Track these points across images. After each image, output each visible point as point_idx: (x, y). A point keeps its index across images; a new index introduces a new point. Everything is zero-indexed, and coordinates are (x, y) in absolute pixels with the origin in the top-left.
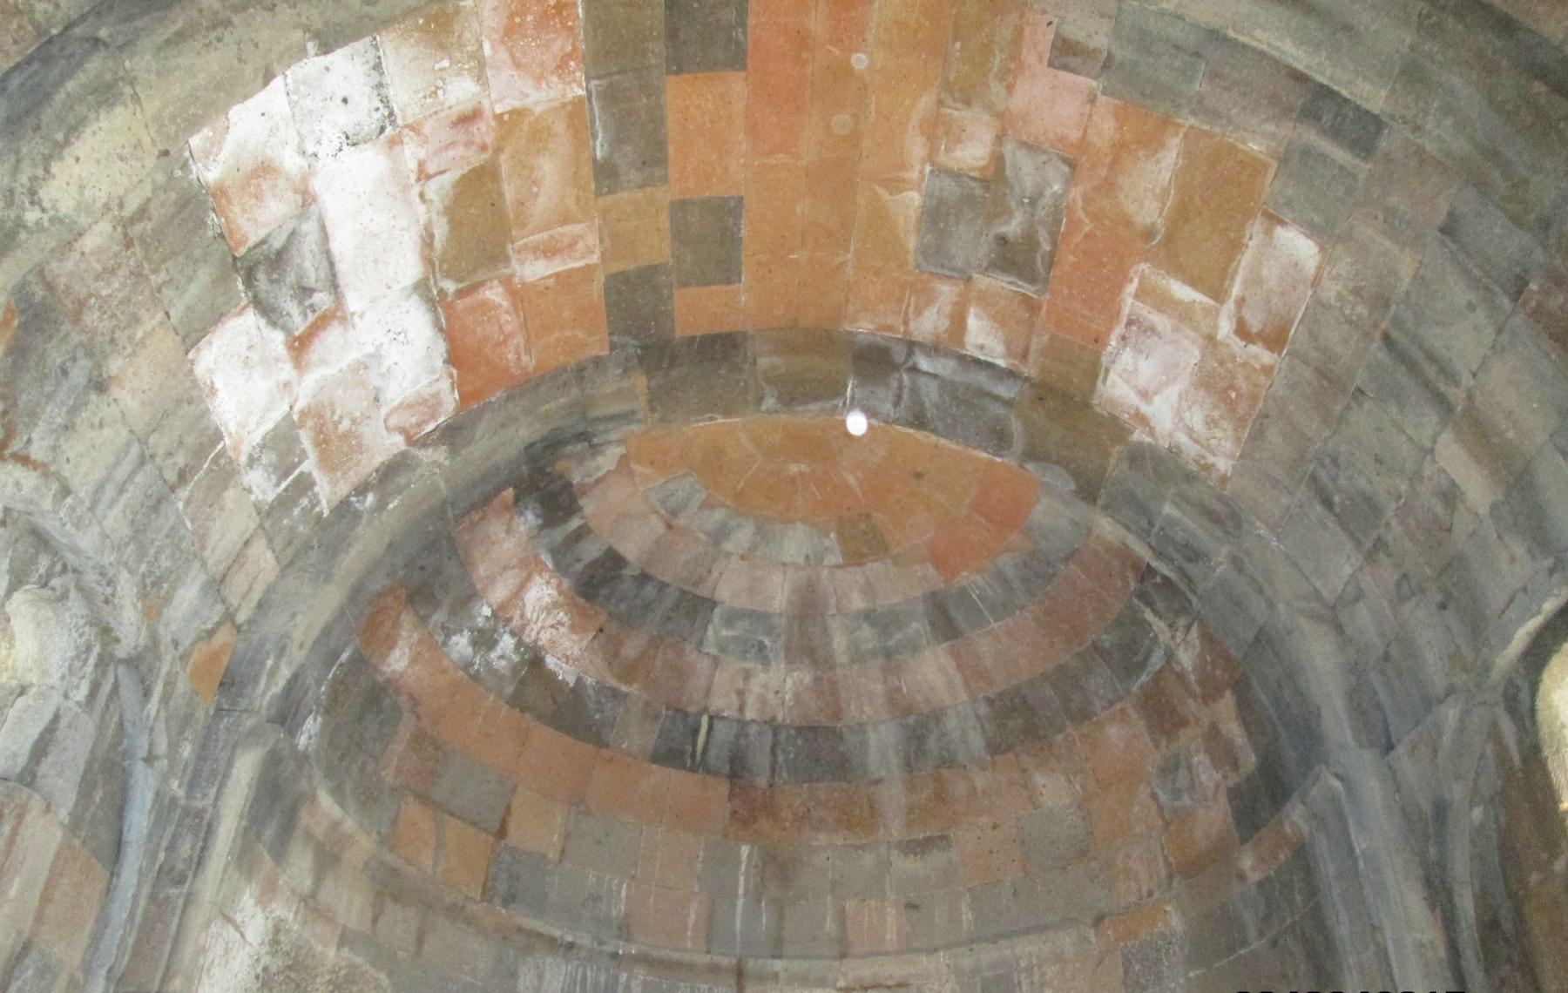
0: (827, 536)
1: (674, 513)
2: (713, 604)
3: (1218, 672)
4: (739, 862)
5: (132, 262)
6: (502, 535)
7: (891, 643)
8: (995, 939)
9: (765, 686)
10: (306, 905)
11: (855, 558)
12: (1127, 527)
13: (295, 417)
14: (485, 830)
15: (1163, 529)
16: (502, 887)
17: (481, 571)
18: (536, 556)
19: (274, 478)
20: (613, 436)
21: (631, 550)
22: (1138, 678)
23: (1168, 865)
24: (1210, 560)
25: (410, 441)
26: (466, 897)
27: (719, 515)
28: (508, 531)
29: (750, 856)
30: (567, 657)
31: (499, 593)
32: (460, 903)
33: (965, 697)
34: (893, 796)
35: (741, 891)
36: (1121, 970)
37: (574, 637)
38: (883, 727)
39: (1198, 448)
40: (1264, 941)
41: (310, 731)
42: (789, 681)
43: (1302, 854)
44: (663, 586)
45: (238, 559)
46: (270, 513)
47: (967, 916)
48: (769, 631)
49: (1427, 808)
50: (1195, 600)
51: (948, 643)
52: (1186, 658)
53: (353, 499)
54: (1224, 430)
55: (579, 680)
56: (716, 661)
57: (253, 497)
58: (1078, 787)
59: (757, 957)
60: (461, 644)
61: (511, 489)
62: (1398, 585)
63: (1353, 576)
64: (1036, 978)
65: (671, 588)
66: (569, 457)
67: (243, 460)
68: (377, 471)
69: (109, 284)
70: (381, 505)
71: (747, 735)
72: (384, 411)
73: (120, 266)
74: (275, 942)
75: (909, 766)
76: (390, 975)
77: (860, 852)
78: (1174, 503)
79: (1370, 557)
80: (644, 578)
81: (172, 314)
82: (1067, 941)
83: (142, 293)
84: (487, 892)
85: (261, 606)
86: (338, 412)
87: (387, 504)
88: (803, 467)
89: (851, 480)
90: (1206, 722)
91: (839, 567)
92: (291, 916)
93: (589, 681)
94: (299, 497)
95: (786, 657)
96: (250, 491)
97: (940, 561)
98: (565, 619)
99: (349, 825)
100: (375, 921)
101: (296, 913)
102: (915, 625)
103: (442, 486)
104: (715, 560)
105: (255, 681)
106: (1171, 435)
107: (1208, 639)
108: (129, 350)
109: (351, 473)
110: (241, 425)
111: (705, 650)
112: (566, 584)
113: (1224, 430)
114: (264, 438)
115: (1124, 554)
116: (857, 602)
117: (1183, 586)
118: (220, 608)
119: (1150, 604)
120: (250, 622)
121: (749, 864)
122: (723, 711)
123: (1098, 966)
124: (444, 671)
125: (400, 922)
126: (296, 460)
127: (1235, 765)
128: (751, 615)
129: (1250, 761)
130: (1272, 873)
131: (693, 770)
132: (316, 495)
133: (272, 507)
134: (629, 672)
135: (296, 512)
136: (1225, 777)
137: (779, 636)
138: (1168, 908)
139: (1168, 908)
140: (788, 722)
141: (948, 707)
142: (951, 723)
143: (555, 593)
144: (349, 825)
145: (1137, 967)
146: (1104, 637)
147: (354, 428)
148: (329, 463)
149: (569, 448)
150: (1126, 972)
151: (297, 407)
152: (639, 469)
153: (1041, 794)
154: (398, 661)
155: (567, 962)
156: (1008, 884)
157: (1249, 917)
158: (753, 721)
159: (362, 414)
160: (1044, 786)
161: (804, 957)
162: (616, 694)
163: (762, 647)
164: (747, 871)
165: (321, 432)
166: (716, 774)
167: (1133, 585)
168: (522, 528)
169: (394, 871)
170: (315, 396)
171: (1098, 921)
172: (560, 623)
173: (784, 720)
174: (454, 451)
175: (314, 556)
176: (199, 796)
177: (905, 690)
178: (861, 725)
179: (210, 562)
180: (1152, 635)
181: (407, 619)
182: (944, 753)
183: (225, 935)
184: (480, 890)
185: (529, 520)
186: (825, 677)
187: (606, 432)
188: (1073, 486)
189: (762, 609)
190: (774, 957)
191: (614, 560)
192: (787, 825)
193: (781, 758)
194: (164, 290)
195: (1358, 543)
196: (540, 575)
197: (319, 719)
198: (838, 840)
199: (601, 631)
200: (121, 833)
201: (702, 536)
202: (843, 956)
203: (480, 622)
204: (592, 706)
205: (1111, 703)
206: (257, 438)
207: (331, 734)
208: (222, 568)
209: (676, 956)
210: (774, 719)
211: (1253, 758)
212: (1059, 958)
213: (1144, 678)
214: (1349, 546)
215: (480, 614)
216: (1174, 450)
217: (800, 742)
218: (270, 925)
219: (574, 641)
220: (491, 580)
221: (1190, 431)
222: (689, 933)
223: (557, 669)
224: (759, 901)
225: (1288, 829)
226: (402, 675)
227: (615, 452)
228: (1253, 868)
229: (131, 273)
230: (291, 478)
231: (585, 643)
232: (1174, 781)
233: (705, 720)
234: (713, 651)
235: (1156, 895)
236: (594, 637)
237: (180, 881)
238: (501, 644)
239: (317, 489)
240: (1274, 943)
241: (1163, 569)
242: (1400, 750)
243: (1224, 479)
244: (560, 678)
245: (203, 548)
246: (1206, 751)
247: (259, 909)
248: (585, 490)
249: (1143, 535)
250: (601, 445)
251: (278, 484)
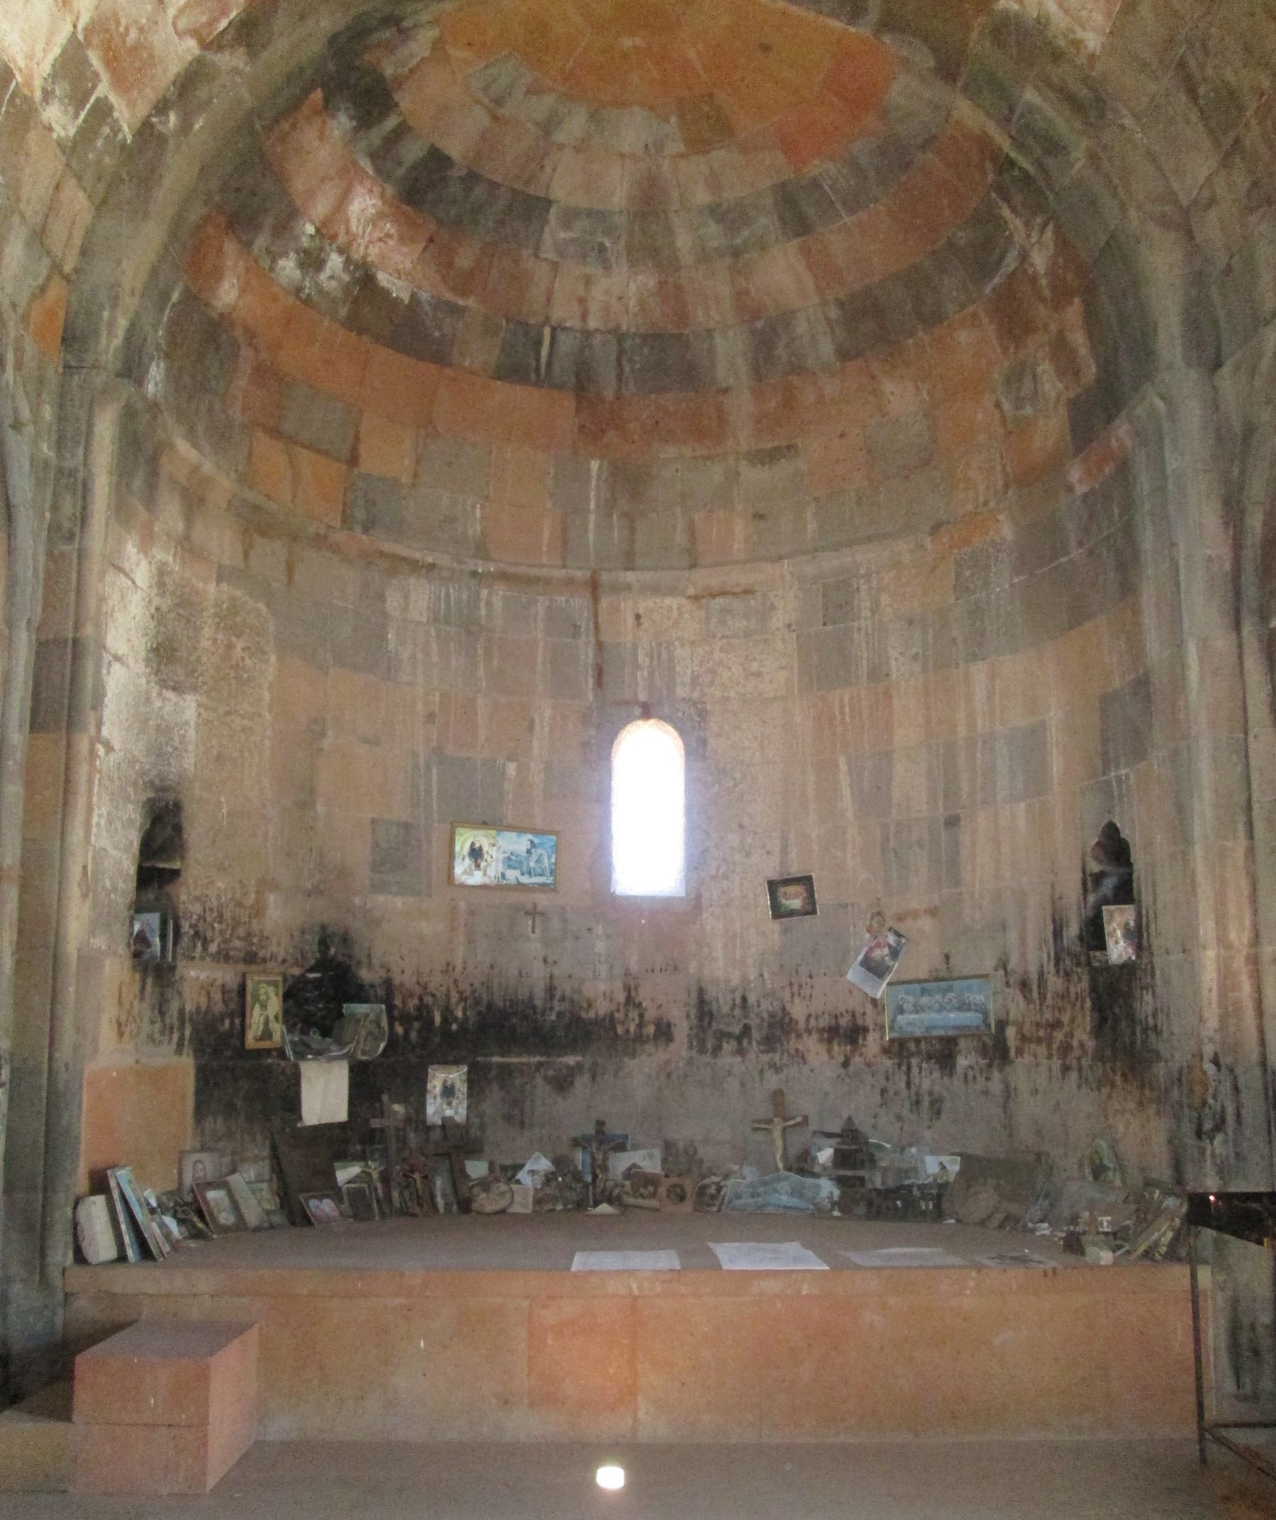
0: (667, 120)
1: (499, 102)
2: (549, 203)
3: (1069, 276)
4: (588, 480)
6: (316, 143)
7: (738, 241)
8: (837, 547)
9: (607, 292)
10: (182, 546)
11: (698, 145)
12: (988, 114)
13: (81, 37)
14: (338, 460)
15: (1022, 116)
16: (360, 514)
17: (299, 184)
18: (355, 163)
19: (71, 110)
20: (424, 17)
21: (455, 149)
22: (992, 278)
23: (1006, 475)
24: (1068, 154)
25: (205, 45)
26: (329, 527)
27: (549, 100)
28: (321, 138)
29: (600, 468)
30: (399, 273)
31: (321, 207)
32: (322, 532)
33: (815, 299)
34: (741, 406)
35: (592, 506)
36: (953, 575)
37: (405, 250)
38: (731, 333)
39: (1068, 19)
40: (1081, 551)
41: (156, 377)
42: (633, 286)
44: (495, 185)
45: (52, 207)
46: (72, 149)
47: (812, 526)
48: (609, 231)
49: (1238, 430)
51: (799, 239)
52: (1039, 261)
53: (154, 120)
55: (413, 295)
56: (555, 266)
57: (55, 135)
58: (925, 396)
59: (610, 570)
60: (288, 267)
61: (319, 90)
62: (1249, 192)
64: (874, 584)
65: (503, 189)
66: (378, 45)
67: (38, 94)
68: (174, 83)
70: (185, 127)
71: (591, 346)
72: (171, 12)
74: (161, 585)
75: (757, 373)
76: (267, 605)
77: (709, 463)
78: (1036, 87)
79: (1226, 162)
80: (472, 178)
82: (903, 547)
84: (347, 520)
85: (84, 252)
86: (124, 21)
87: (192, 125)
88: (638, 41)
89: (692, 53)
90: (1053, 328)
91: (682, 156)
92: (170, 559)
93: (424, 296)
94: (100, 125)
95: (629, 260)
96: (50, 129)
97: (789, 147)
98: (393, 231)
99: (208, 467)
100: (246, 555)
101: (175, 555)
102: (763, 220)
103: (246, 96)
104: (546, 154)
105: (96, 333)
107: (1063, 243)
109: (148, 90)
110: (30, 57)
111: (543, 255)
112: (390, 190)
114: (53, 66)
115: (983, 142)
116: (702, 196)
117: (1041, 183)
118: (46, 262)
119: (1007, 199)
120: (76, 271)
121: (599, 478)
122: (565, 320)
123: (932, 572)
124: (275, 299)
125: (270, 554)
126: (90, 85)
127: (1077, 373)
128: (590, 213)
129: (1091, 371)
131: (538, 383)
132: (116, 121)
133: (75, 144)
134: (464, 284)
135: (100, 143)
136: (1067, 388)
137: (619, 237)
138: (1001, 517)
139: (1001, 517)
140: (633, 330)
141: (799, 310)
142: (801, 328)
143: (379, 203)
144: (208, 467)
145: (968, 573)
146: (960, 234)
147: (142, 38)
148: (120, 82)
149: (377, 36)
150: (957, 579)
151: (81, 25)
152: (456, 53)
153: (889, 402)
154: (227, 294)
155: (430, 583)
156: (853, 494)
157: (1071, 527)
158: (597, 330)
159: (148, 20)
160: (892, 393)
161: (656, 569)
162: (454, 310)
163: (602, 248)
164: (598, 486)
165: (109, 48)
166: (560, 387)
167: (991, 177)
168: (336, 132)
169: (256, 508)
170: (96, 8)
171: (936, 529)
172: (388, 235)
173: (628, 330)
174: (253, 54)
175: (126, 192)
176: (68, 456)
177: (753, 291)
178: (709, 332)
179: (28, 214)
180: (1007, 233)
181: (230, 247)
182: (793, 359)
183: (118, 583)
184: (339, 518)
185: (341, 124)
186: (671, 280)
187: (416, 12)
188: (932, 64)
189: (601, 207)
190: (627, 569)
191: (437, 160)
192: (636, 437)
193: (627, 368)
195: (1217, 144)
196: (361, 183)
197: (162, 364)
198: (687, 452)
199: (431, 240)
200: (7, 498)
201: (529, 125)
202: (693, 566)
203: (305, 242)
204: (429, 323)
205: (963, 306)
206: (46, 68)
207: (174, 378)
208: (39, 219)
209: (535, 572)
210: (618, 328)
211: (1094, 369)
212: (897, 565)
213: (996, 280)
214: (1207, 144)
215: (303, 233)
216: (1043, 21)
217: (646, 351)
218: (154, 570)
219: (405, 255)
220: (311, 193)
222: (544, 549)
223: (389, 286)
224: (609, 515)
225: (1114, 443)
226: (234, 308)
227: (427, 35)
228: (1080, 481)
230: (88, 106)
231: (416, 255)
232: (1019, 389)
233: (547, 331)
234: (551, 256)
235: (992, 504)
236: (425, 249)
237: (70, 537)
238: (329, 264)
239: (116, 114)
240: (1091, 553)
241: (1024, 162)
242: (1226, 370)
243: (1092, 57)
244: (394, 295)
245: (18, 200)
246: (1051, 360)
247: (142, 556)
248: (399, 82)
249: (1004, 122)
250: (410, 29)
251: (76, 116)
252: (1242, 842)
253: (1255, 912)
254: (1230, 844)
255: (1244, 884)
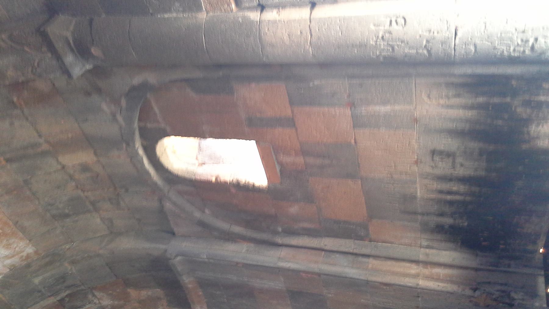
15: (44, 288)
43: (203, 284)
50: (83, 287)
54: (14, 242)
63: (102, 219)
79: (96, 210)
106: (4, 266)
107: (103, 289)
113: (14, 242)
127: (159, 299)
129: (159, 292)
130: (205, 300)
136: (162, 305)
195: (89, 211)
221: (7, 257)
241: (64, 294)
242: (176, 230)
243: (36, 252)
252: (371, 260)
253: (403, 260)
254: (370, 266)
255: (389, 263)
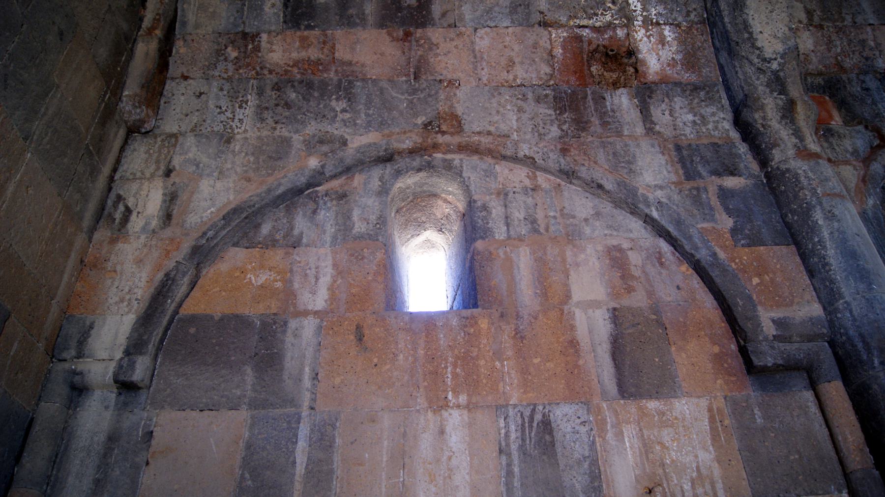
5: (831, 30)
69: (836, 46)
73: (830, 37)
81: (872, 22)
83: (851, 32)
108: (877, 53)
194: (856, 20)
229: (837, 33)
